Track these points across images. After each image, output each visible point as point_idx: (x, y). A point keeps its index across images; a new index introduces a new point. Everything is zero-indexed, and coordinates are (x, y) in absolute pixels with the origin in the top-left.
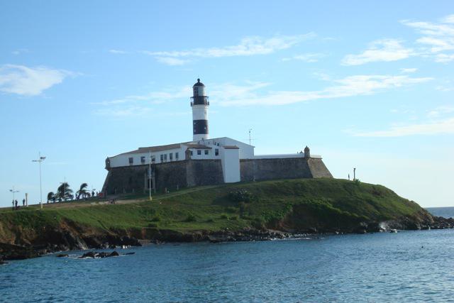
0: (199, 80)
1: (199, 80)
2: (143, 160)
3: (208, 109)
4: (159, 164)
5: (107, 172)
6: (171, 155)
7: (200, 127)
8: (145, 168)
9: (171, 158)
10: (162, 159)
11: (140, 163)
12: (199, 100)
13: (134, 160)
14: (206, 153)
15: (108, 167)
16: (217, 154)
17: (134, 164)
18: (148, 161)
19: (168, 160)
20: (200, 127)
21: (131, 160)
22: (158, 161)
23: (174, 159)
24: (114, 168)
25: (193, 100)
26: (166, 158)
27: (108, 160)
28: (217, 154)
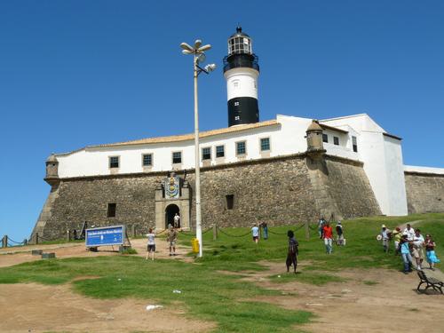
8: (150, 179)
11: (140, 169)
14: (336, 142)
16: (355, 149)
17: (122, 170)
19: (231, 157)
23: (254, 152)
26: (220, 153)
28: (355, 149)
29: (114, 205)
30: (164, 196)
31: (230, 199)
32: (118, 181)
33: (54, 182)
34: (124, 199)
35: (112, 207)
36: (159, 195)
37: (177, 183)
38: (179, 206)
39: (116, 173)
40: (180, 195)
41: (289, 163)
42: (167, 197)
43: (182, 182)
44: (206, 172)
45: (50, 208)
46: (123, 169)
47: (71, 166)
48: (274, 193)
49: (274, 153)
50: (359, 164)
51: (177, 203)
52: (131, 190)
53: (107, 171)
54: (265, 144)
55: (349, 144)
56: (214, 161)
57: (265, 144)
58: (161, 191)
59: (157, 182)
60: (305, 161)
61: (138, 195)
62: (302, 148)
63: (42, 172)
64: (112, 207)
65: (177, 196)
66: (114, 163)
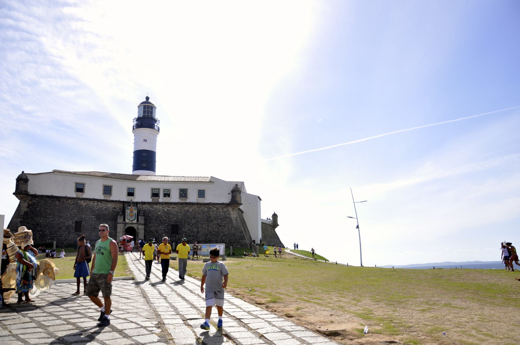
0: (147, 98)
1: (147, 98)
2: (107, 190)
3: (160, 138)
4: (143, 203)
5: (16, 202)
7: (144, 159)
8: (109, 205)
10: (155, 195)
11: (101, 197)
12: (146, 119)
13: (86, 190)
15: (18, 193)
19: (175, 198)
20: (144, 159)
23: (193, 197)
24: (35, 196)
27: (22, 180)
29: (80, 222)
30: (124, 220)
36: (120, 220)
37: (135, 211)
38: (136, 228)
39: (81, 197)
40: (138, 221)
41: (217, 208)
42: (127, 221)
44: (155, 206)
45: (19, 220)
46: (88, 194)
48: (208, 226)
49: (208, 199)
51: (135, 226)
53: (72, 194)
54: (201, 193)
56: (162, 199)
57: (201, 193)
58: (122, 217)
59: (115, 208)
61: (101, 217)
62: (227, 199)
65: (135, 221)
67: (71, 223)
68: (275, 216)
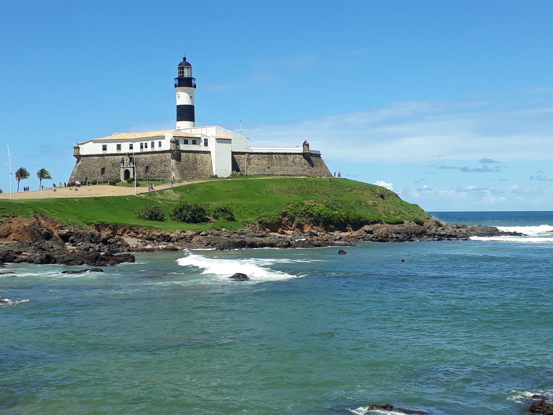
0: (185, 59)
1: (185, 59)
6: (153, 143)
8: (121, 157)
9: (153, 146)
10: (142, 147)
11: (115, 151)
16: (206, 144)
18: (125, 148)
19: (149, 149)
21: (105, 148)
22: (137, 148)
23: (157, 148)
25: (177, 82)
26: (146, 147)
31: (147, 167)
32: (107, 157)
33: (79, 157)
34: (108, 165)
35: (103, 169)
36: (122, 166)
37: (129, 160)
42: (125, 166)
43: (131, 159)
46: (109, 151)
47: (85, 150)
50: (209, 152)
51: (129, 169)
52: (111, 161)
53: (101, 152)
55: (202, 143)
56: (145, 150)
57: (160, 145)
60: (170, 154)
63: (73, 152)
64: (103, 169)
66: (105, 148)
67: (99, 170)
68: (306, 145)
